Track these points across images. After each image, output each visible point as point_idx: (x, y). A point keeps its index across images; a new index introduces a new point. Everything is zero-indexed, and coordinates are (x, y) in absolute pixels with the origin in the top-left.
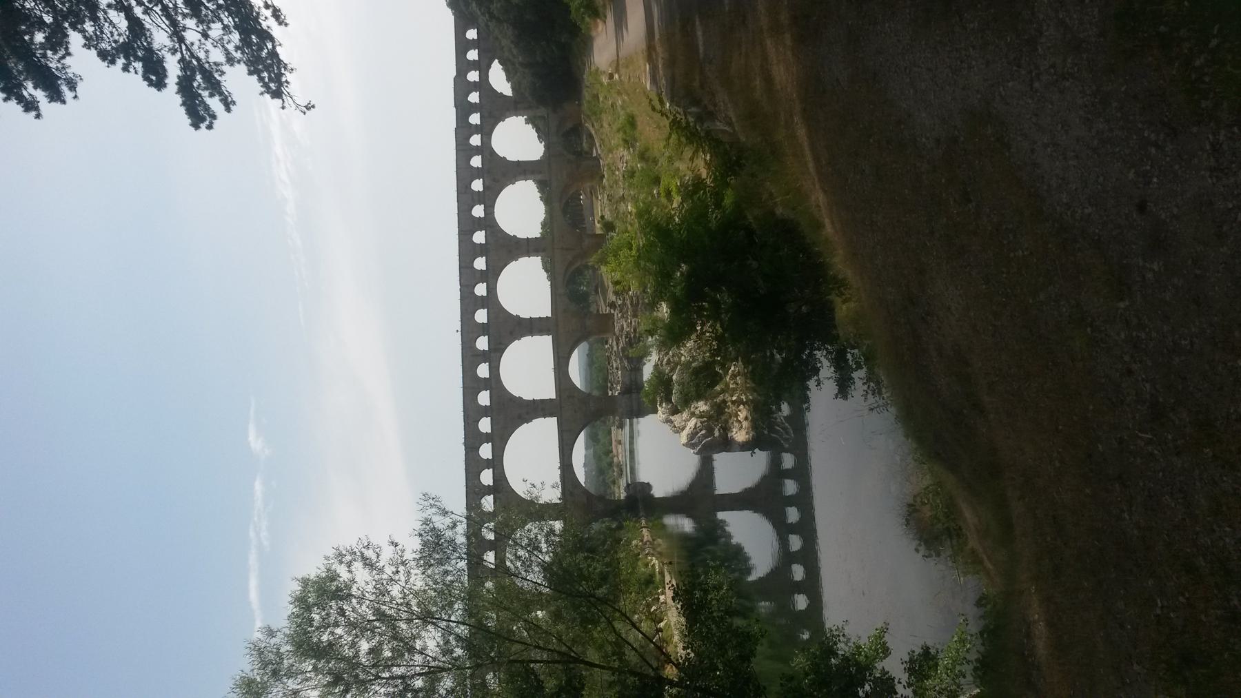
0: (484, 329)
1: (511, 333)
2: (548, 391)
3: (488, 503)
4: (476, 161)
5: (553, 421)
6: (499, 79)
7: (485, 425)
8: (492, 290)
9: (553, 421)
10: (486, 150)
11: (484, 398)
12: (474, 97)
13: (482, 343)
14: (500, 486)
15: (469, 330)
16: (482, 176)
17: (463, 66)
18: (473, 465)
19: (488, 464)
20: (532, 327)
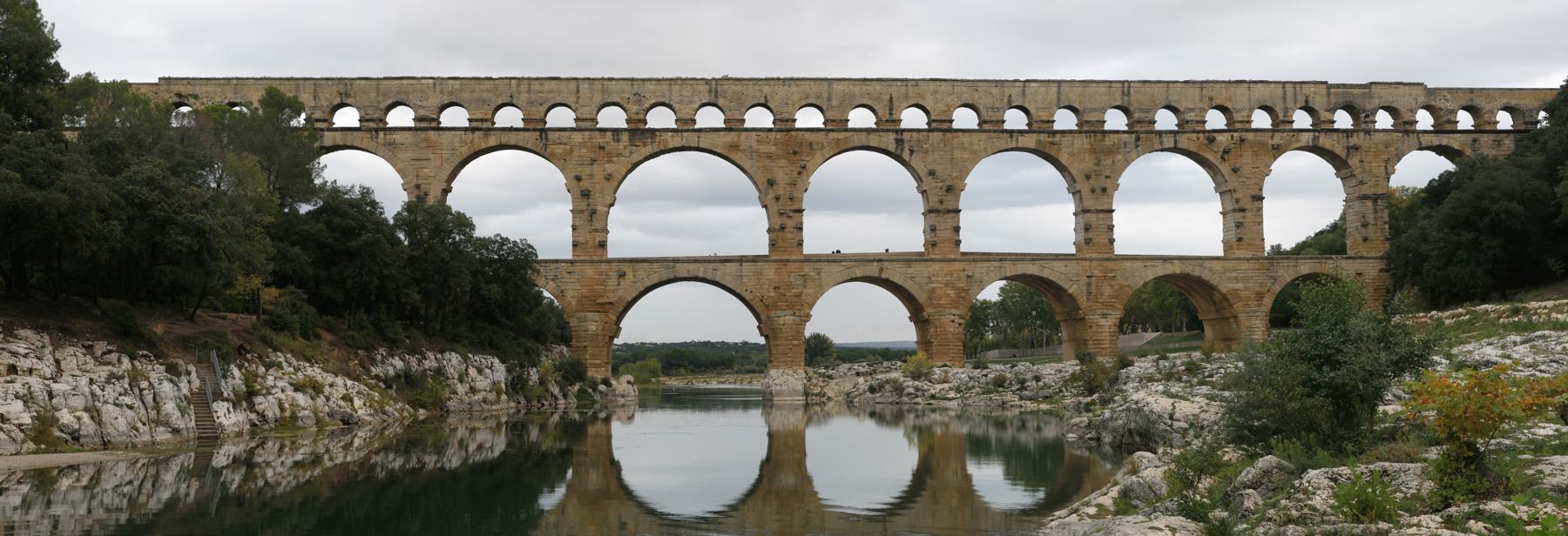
0: (940, 125)
1: (932, 173)
3: (612, 118)
4: (1261, 120)
5: (759, 244)
6: (1418, 169)
7: (759, 118)
8: (1013, 141)
9: (759, 244)
10: (1281, 139)
11: (809, 118)
12: (1384, 120)
14: (642, 141)
16: (1229, 135)
17: (1433, 99)
19: (686, 123)
20: (942, 208)
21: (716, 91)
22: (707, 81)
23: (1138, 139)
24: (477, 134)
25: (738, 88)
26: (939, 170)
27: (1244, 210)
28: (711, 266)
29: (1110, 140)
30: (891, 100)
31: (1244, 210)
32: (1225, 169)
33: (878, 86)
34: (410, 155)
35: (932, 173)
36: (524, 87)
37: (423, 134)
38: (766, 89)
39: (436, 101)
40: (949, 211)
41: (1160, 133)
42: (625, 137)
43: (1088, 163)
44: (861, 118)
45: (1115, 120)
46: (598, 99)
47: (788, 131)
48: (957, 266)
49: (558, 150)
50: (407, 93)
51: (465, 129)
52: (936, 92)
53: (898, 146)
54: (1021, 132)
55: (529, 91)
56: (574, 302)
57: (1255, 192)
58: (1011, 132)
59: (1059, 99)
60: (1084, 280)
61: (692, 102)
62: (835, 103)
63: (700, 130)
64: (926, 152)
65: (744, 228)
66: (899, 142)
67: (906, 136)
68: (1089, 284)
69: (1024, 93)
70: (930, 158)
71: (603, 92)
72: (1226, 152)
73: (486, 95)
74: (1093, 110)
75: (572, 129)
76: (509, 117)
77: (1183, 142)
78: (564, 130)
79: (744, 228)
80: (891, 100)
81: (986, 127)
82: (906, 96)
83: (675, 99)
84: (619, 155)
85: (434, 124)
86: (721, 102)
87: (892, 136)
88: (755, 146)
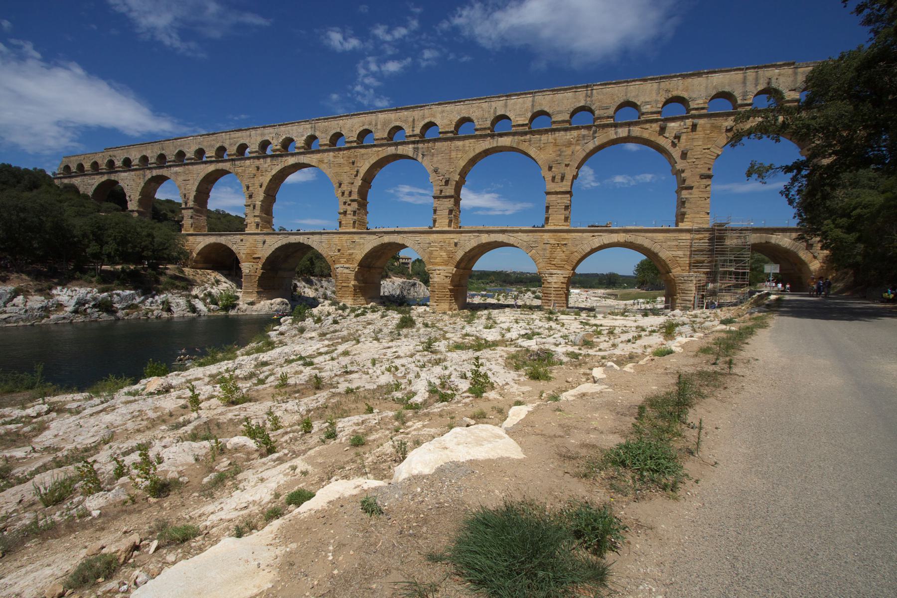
1: (436, 171)
26: (440, 166)
27: (691, 188)
31: (691, 188)
32: (676, 153)
33: (406, 113)
34: (183, 178)
35: (436, 171)
36: (228, 137)
40: (446, 197)
48: (452, 236)
50: (183, 146)
52: (443, 112)
56: (244, 256)
57: (705, 171)
59: (533, 106)
61: (303, 136)
62: (379, 127)
64: (433, 155)
66: (416, 150)
69: (506, 106)
70: (435, 159)
71: (262, 135)
72: (678, 137)
77: (636, 131)
81: (477, 133)
82: (423, 118)
84: (266, 171)
86: (317, 134)
88: (332, 159)
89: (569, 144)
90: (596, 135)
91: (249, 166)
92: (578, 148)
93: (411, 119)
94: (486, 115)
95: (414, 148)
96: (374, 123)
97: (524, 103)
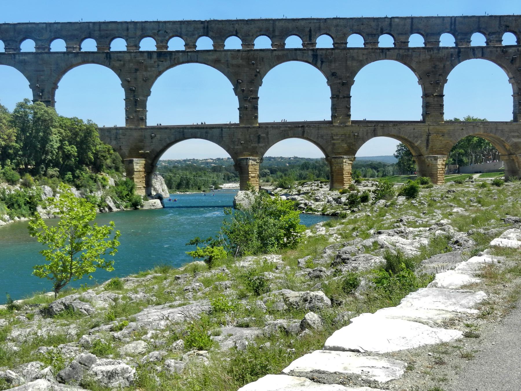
1: (334, 74)
2: (267, 113)
3: (148, 44)
5: (235, 119)
7: (233, 43)
9: (235, 119)
11: (263, 43)
13: (324, 42)
14: (166, 59)
15: (339, 27)
18: (190, 30)
21: (207, 28)
22: (202, 22)
23: (459, 52)
24: (70, 56)
25: (221, 26)
28: (204, 130)
29: (442, 54)
30: (310, 31)
36: (97, 28)
37: (40, 56)
38: (236, 26)
39: (46, 36)
41: (474, 49)
42: (155, 56)
43: (428, 66)
44: (294, 42)
45: (447, 40)
46: (139, 33)
47: (248, 51)
49: (117, 64)
51: (64, 53)
52: (337, 26)
53: (316, 58)
54: (389, 49)
55: (100, 30)
58: (382, 49)
60: (424, 137)
62: (277, 33)
63: (198, 51)
64: (331, 62)
65: (226, 110)
67: (319, 53)
68: (428, 140)
69: (390, 25)
70: (333, 65)
73: (76, 33)
74: (433, 34)
75: (124, 52)
76: (89, 45)
78: (120, 52)
79: (226, 110)
80: (310, 31)
81: (368, 46)
83: (184, 31)
84: (152, 66)
85: (46, 50)
87: (310, 53)
89: (441, 60)
90: (460, 54)
91: (130, 61)
92: (448, 63)
93: (308, 29)
94: (375, 32)
95: (313, 55)
96: (271, 29)
97: (405, 25)
